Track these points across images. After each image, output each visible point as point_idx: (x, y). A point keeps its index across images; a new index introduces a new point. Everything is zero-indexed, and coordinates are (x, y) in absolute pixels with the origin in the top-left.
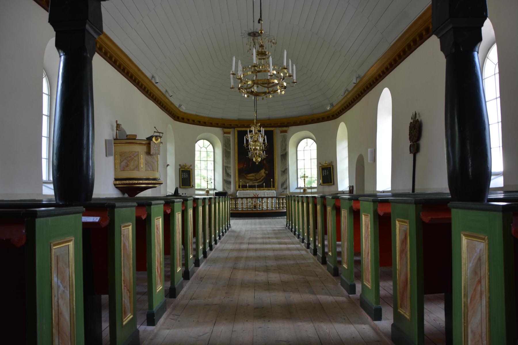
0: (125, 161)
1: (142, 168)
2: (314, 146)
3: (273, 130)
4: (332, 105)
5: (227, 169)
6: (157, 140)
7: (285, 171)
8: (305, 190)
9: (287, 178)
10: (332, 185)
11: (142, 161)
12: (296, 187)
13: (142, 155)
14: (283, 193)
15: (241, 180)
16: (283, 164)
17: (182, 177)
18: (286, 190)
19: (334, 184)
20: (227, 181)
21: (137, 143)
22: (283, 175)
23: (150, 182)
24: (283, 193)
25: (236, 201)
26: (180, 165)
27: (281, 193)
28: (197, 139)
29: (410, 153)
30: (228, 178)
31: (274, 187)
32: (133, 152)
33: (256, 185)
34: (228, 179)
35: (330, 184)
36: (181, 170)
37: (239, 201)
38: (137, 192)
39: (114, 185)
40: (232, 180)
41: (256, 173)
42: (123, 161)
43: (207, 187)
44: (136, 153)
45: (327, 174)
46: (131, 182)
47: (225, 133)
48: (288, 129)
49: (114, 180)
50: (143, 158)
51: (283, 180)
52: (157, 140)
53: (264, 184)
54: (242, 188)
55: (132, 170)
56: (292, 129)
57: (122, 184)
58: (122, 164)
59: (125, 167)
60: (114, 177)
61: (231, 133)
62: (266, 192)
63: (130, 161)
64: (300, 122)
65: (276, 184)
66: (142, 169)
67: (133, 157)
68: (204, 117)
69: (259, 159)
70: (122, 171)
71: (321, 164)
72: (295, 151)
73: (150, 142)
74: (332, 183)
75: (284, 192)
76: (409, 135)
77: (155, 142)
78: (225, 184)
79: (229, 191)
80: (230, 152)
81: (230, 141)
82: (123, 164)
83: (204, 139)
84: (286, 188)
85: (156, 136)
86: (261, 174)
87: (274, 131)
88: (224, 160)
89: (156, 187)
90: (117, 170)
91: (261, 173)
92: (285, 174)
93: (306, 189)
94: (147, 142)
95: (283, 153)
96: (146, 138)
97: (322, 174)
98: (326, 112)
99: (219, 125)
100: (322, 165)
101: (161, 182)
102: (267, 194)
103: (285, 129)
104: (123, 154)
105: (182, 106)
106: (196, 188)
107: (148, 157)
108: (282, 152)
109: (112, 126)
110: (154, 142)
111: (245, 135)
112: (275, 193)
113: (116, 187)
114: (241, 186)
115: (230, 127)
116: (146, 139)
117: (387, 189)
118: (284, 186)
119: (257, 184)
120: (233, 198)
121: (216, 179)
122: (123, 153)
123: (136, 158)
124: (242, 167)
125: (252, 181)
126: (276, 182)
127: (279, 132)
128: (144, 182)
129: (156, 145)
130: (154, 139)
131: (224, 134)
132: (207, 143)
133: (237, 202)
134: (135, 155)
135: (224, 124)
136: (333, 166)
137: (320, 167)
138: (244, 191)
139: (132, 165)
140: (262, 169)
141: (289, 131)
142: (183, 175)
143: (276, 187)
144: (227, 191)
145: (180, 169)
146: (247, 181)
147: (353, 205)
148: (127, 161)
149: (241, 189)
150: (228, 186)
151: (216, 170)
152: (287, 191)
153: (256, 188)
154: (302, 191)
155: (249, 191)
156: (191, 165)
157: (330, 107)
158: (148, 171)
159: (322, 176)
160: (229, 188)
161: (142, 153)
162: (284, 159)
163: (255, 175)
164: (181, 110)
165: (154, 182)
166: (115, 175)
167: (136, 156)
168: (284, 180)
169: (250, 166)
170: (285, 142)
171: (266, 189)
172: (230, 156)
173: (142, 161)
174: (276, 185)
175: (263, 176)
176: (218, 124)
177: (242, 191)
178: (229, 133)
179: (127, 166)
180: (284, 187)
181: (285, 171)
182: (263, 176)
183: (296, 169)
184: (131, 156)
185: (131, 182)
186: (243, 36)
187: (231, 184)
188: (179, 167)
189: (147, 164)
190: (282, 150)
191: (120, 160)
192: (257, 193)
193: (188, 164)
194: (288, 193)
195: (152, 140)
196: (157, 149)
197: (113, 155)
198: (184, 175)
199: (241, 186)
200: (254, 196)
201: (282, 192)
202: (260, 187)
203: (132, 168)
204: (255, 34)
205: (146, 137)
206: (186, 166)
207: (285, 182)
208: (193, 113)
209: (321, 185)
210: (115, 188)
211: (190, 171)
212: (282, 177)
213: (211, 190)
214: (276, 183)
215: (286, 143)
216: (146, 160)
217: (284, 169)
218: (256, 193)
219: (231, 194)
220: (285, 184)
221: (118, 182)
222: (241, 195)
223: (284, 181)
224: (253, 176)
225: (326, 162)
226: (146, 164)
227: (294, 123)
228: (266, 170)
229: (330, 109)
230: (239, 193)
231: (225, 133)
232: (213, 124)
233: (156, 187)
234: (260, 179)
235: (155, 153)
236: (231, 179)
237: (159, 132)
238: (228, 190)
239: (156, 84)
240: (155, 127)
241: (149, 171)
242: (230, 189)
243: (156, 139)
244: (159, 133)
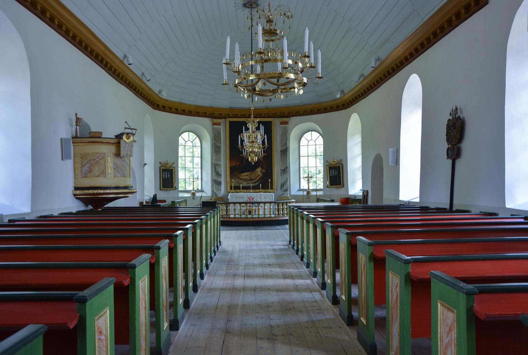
0: (88, 165)
1: (110, 174)
2: (320, 141)
3: (271, 120)
4: (342, 92)
5: (216, 167)
6: (128, 138)
7: (285, 170)
8: (308, 193)
9: (287, 178)
10: (340, 187)
11: (109, 165)
13: (109, 158)
14: (282, 196)
15: (233, 180)
16: (282, 161)
17: (163, 177)
18: (286, 193)
19: (343, 186)
20: (217, 182)
21: (103, 142)
22: (283, 174)
23: (120, 191)
24: (282, 196)
25: (227, 208)
26: (160, 163)
27: (281, 196)
28: (181, 131)
29: (447, 159)
30: (218, 177)
31: (272, 188)
32: (98, 153)
33: (250, 186)
34: (218, 179)
35: (340, 186)
36: (162, 168)
37: (231, 207)
38: (104, 203)
39: (73, 196)
40: (222, 180)
41: (251, 172)
42: (85, 165)
43: (193, 189)
45: (335, 174)
46: (95, 192)
47: (214, 124)
48: (289, 120)
49: (74, 189)
50: (110, 161)
51: (283, 180)
52: (128, 138)
53: (261, 184)
54: (234, 189)
55: (97, 177)
56: (294, 119)
57: (83, 195)
58: (83, 169)
59: (88, 173)
60: (74, 185)
61: (222, 124)
62: (262, 194)
63: (94, 165)
64: (304, 112)
65: (275, 186)
66: (110, 176)
67: (98, 159)
68: (190, 106)
69: (256, 159)
70: (83, 177)
71: (329, 162)
72: (297, 146)
73: (120, 140)
74: (341, 185)
75: (284, 195)
76: (446, 136)
77: (127, 141)
78: (214, 185)
79: (219, 193)
80: (220, 146)
81: (220, 134)
82: (86, 168)
83: (189, 131)
84: (286, 190)
85: (128, 134)
86: (256, 174)
87: (272, 122)
88: (213, 156)
89: (128, 197)
90: (77, 176)
91: (257, 172)
92: (285, 173)
93: (310, 191)
94: (116, 141)
95: (283, 149)
96: (115, 136)
97: (330, 175)
98: (335, 100)
99: (208, 114)
100: (329, 163)
101: (135, 190)
102: (264, 198)
103: (285, 119)
104: (85, 156)
105: (163, 92)
106: (180, 189)
107: (117, 160)
108: (282, 148)
109: (71, 120)
111: (240, 135)
112: (273, 196)
113: (77, 198)
114: (233, 187)
115: (220, 117)
116: (115, 137)
117: (412, 200)
118: (284, 188)
119: (253, 185)
120: (224, 203)
121: (203, 179)
122: (85, 154)
123: (102, 162)
124: (235, 164)
125: (246, 181)
126: (274, 183)
127: (279, 123)
128: (112, 191)
129: (127, 145)
130: (124, 137)
131: (213, 125)
132: (192, 136)
133: (228, 208)
134: (100, 157)
135: (214, 114)
136: (342, 165)
137: (327, 165)
138: (237, 194)
139: (96, 170)
140: (258, 167)
142: (164, 175)
143: (274, 188)
144: (216, 193)
145: (160, 167)
146: (240, 181)
147: (410, 271)
148: (90, 165)
149: (233, 191)
150: (218, 187)
151: (203, 168)
152: (287, 194)
153: (251, 190)
154: (305, 193)
155: (242, 194)
156: (174, 163)
157: (341, 94)
158: (117, 178)
159: (330, 177)
160: (219, 190)
161: (109, 155)
162: (284, 155)
163: (250, 174)
164: (163, 97)
165: (125, 191)
166: (75, 183)
168: (284, 181)
169: (244, 163)
170: (285, 136)
171: (262, 190)
172: (220, 152)
173: (109, 165)
174: (275, 186)
175: (259, 175)
176: (206, 113)
177: (235, 194)
179: (90, 172)
180: (284, 189)
181: (285, 169)
182: (259, 175)
183: (298, 167)
185: (95, 192)
186: (237, 8)
187: (221, 185)
188: (159, 165)
189: (116, 168)
190: (282, 145)
191: (82, 164)
192: (252, 196)
193: (170, 162)
194: (288, 196)
195: (122, 139)
196: (128, 149)
197: (71, 159)
198: (165, 175)
199: (233, 187)
200: (249, 201)
201: (281, 194)
202: (256, 188)
203: (97, 173)
204: (251, 5)
205: (115, 135)
206: (167, 164)
207: (285, 183)
208: (177, 100)
209: (328, 187)
210: (75, 199)
211: (172, 170)
212: (282, 177)
213: (198, 191)
214: (274, 184)
215: (287, 136)
216: (114, 164)
217: (284, 167)
218: (251, 196)
219: (221, 196)
220: (285, 185)
221: (78, 192)
222: (232, 198)
223: (284, 182)
224: (248, 176)
225: (334, 160)
226: (114, 168)
227: (296, 112)
229: (339, 97)
230: (231, 195)
231: (214, 124)
232: (200, 113)
233: (128, 197)
234: (256, 179)
235: (126, 155)
236: (221, 179)
237: (131, 128)
238: (218, 192)
239: (129, 66)
240: (126, 122)
241: (119, 177)
242: (220, 191)
243: (127, 136)
244: (132, 129)
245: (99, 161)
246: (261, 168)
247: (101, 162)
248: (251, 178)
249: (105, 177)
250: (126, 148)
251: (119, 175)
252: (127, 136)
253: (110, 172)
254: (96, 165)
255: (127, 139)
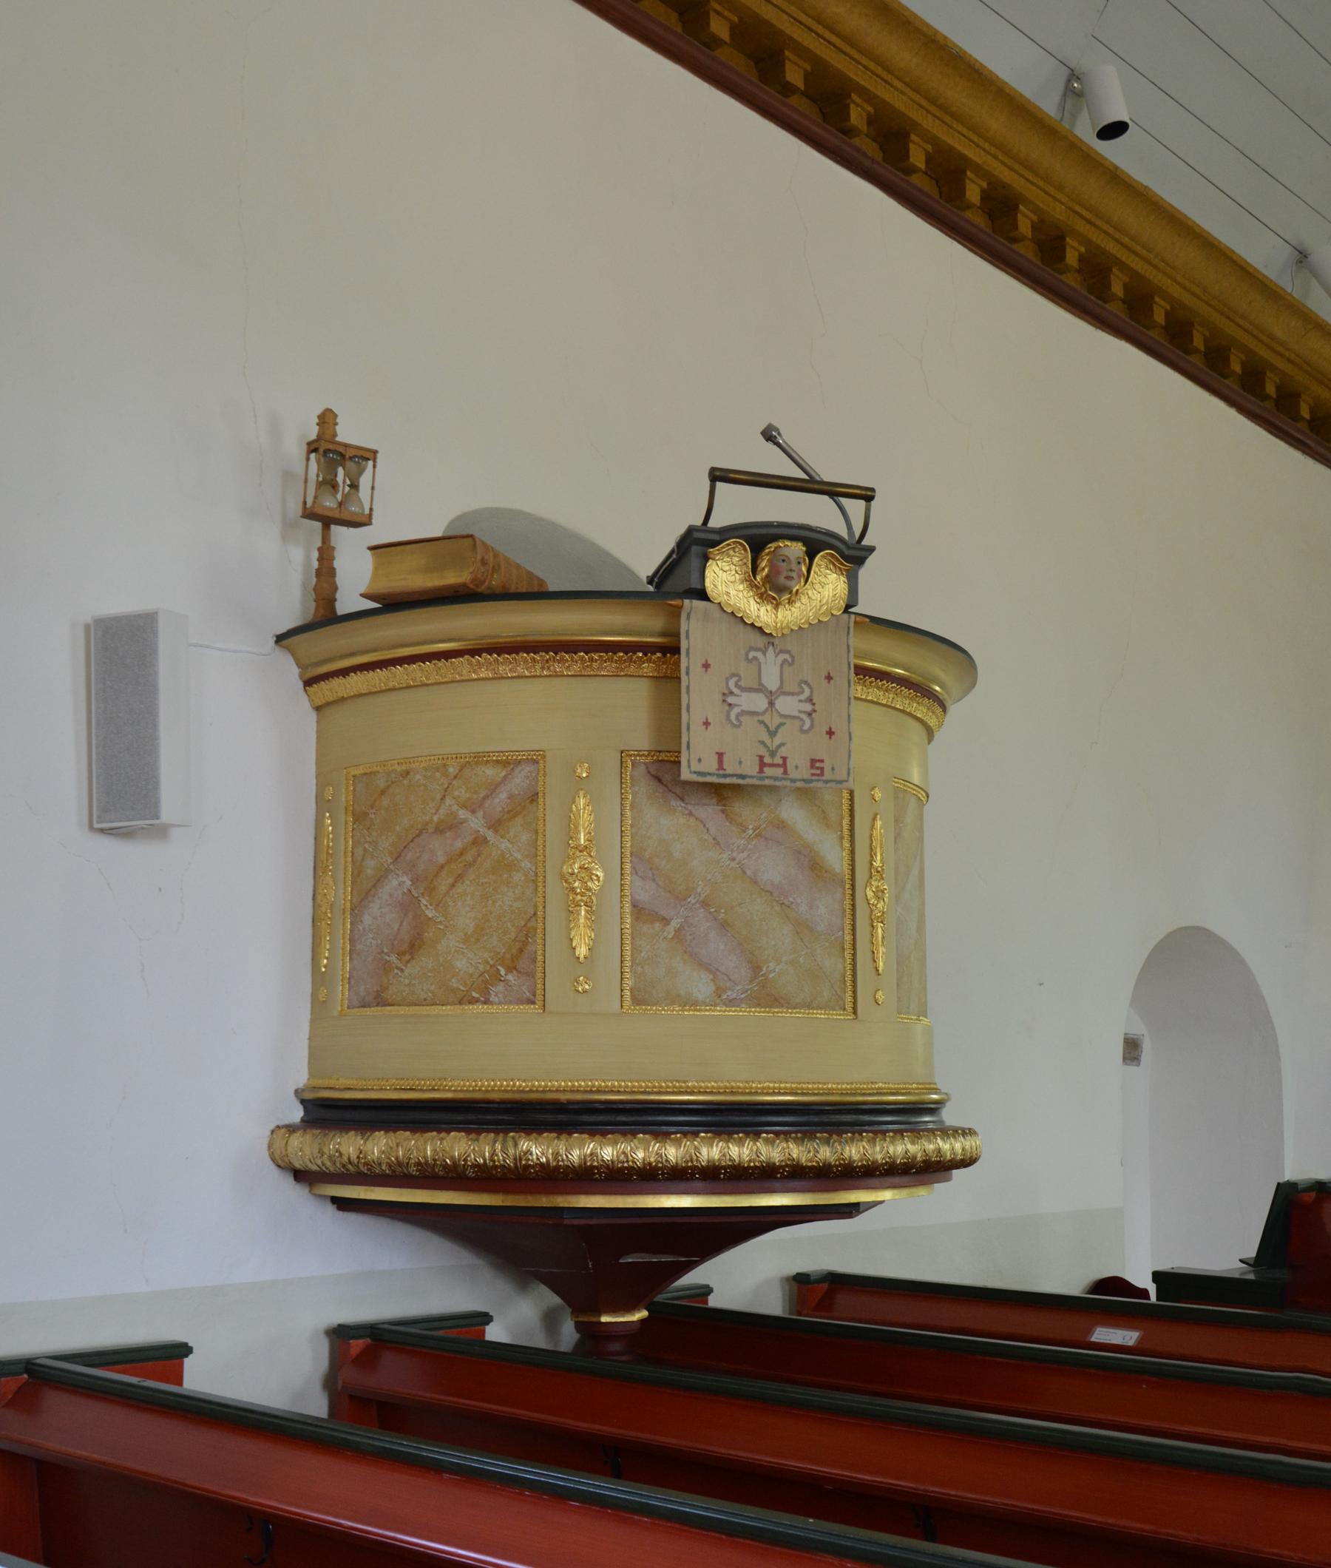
0: (398, 883)
32: (479, 759)
42: (378, 881)
44: (520, 779)
49: (296, 1114)
58: (367, 920)
63: (444, 883)
70: (364, 1005)
101: (949, 1147)
110: (738, 619)
113: (343, 1204)
122: (382, 783)
123: (511, 844)
148: (415, 881)
167: (512, 814)
179: (413, 947)
184: (462, 814)
185: (537, 1149)
195: (702, 595)
203: (467, 963)
226: (640, 912)
235: (750, 768)
239: (1107, 149)
240: (770, 435)
241: (694, 1004)
243: (755, 570)
244: (834, 491)
245: (490, 835)
247: (505, 845)
249: (849, 1006)
250: (760, 689)
251: (701, 986)
252: (755, 570)
253: (582, 951)
254: (460, 878)
255: (763, 597)
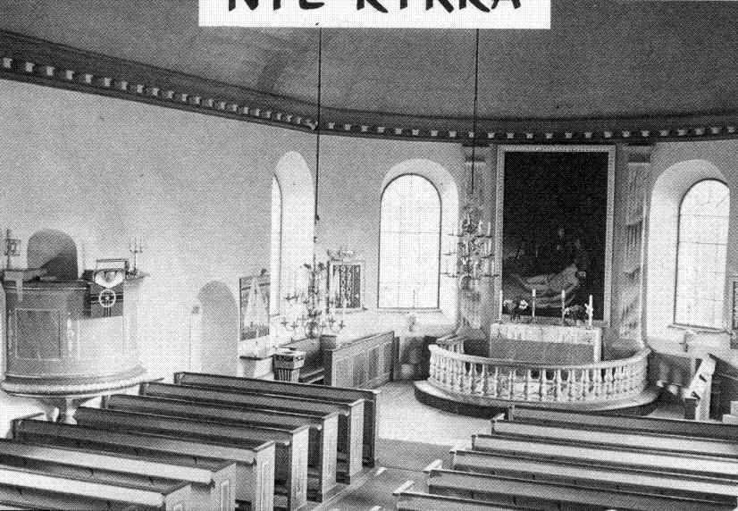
6: (108, 280)
12: (670, 321)
31: (598, 315)
56: (666, 148)
103: (644, 150)
115: (481, 140)
140: (569, 264)
141: (655, 156)
178: (482, 159)
213: (424, 310)
228: (579, 267)
246: (577, 266)
248: (551, 290)
